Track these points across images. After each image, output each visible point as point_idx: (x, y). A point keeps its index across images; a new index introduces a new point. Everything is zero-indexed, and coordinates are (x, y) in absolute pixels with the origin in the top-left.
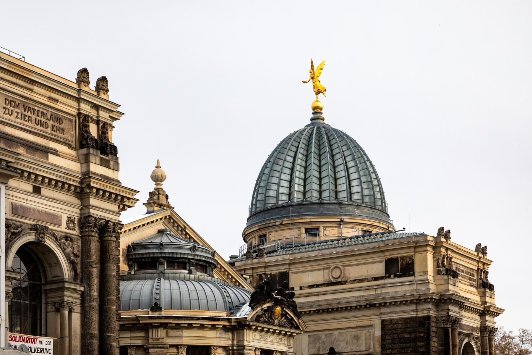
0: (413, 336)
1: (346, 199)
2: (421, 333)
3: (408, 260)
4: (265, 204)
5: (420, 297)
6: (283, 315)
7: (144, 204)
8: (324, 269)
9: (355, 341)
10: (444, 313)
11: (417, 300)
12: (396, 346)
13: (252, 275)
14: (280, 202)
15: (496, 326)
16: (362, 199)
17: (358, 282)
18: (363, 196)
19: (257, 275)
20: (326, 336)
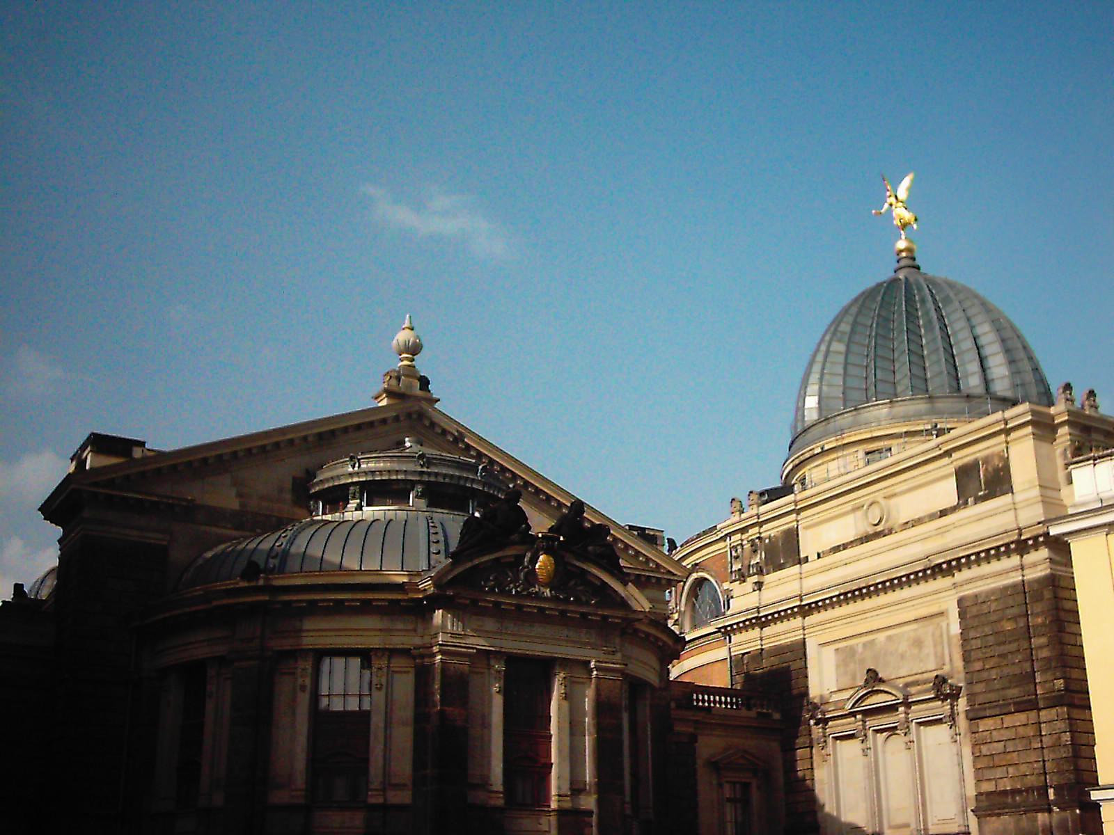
2: (1037, 615)
3: (996, 462)
5: (1021, 535)
7: (373, 398)
8: (855, 509)
9: (915, 651)
11: (1018, 542)
13: (741, 544)
19: (748, 541)
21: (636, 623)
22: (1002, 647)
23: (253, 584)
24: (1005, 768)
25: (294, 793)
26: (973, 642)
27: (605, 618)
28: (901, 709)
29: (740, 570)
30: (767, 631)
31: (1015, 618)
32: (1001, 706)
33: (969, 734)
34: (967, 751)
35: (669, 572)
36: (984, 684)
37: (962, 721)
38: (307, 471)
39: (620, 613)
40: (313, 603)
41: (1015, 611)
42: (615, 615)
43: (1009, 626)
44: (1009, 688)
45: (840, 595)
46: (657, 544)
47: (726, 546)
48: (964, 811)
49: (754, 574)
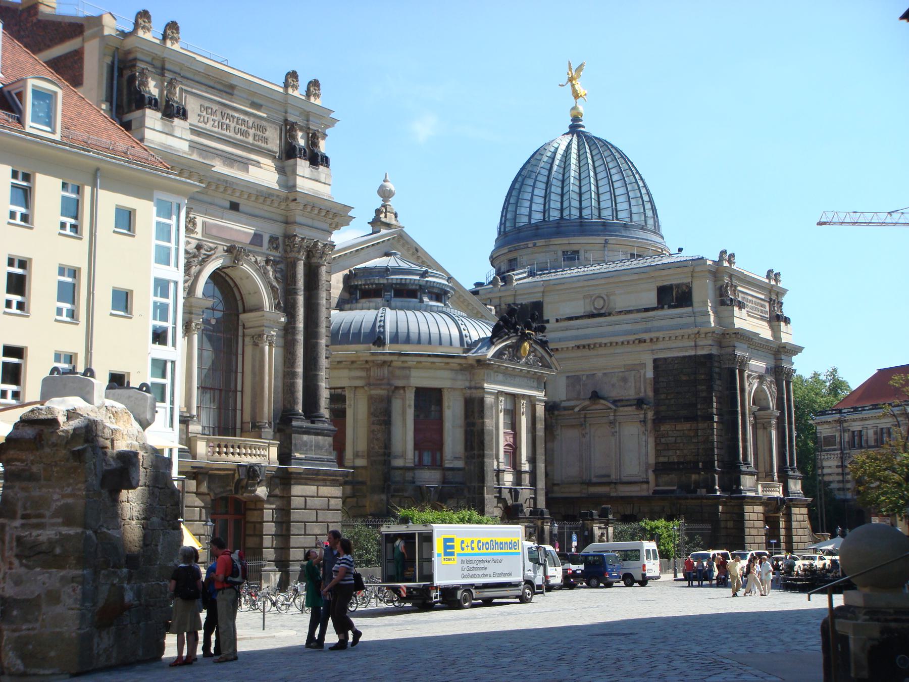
1: (611, 218)
3: (684, 288)
4: (515, 223)
6: (530, 352)
9: (622, 384)
10: (730, 350)
14: (533, 221)
15: (794, 367)
16: (631, 218)
18: (631, 213)
34: (651, 441)
37: (650, 425)
43: (684, 378)
48: (647, 471)
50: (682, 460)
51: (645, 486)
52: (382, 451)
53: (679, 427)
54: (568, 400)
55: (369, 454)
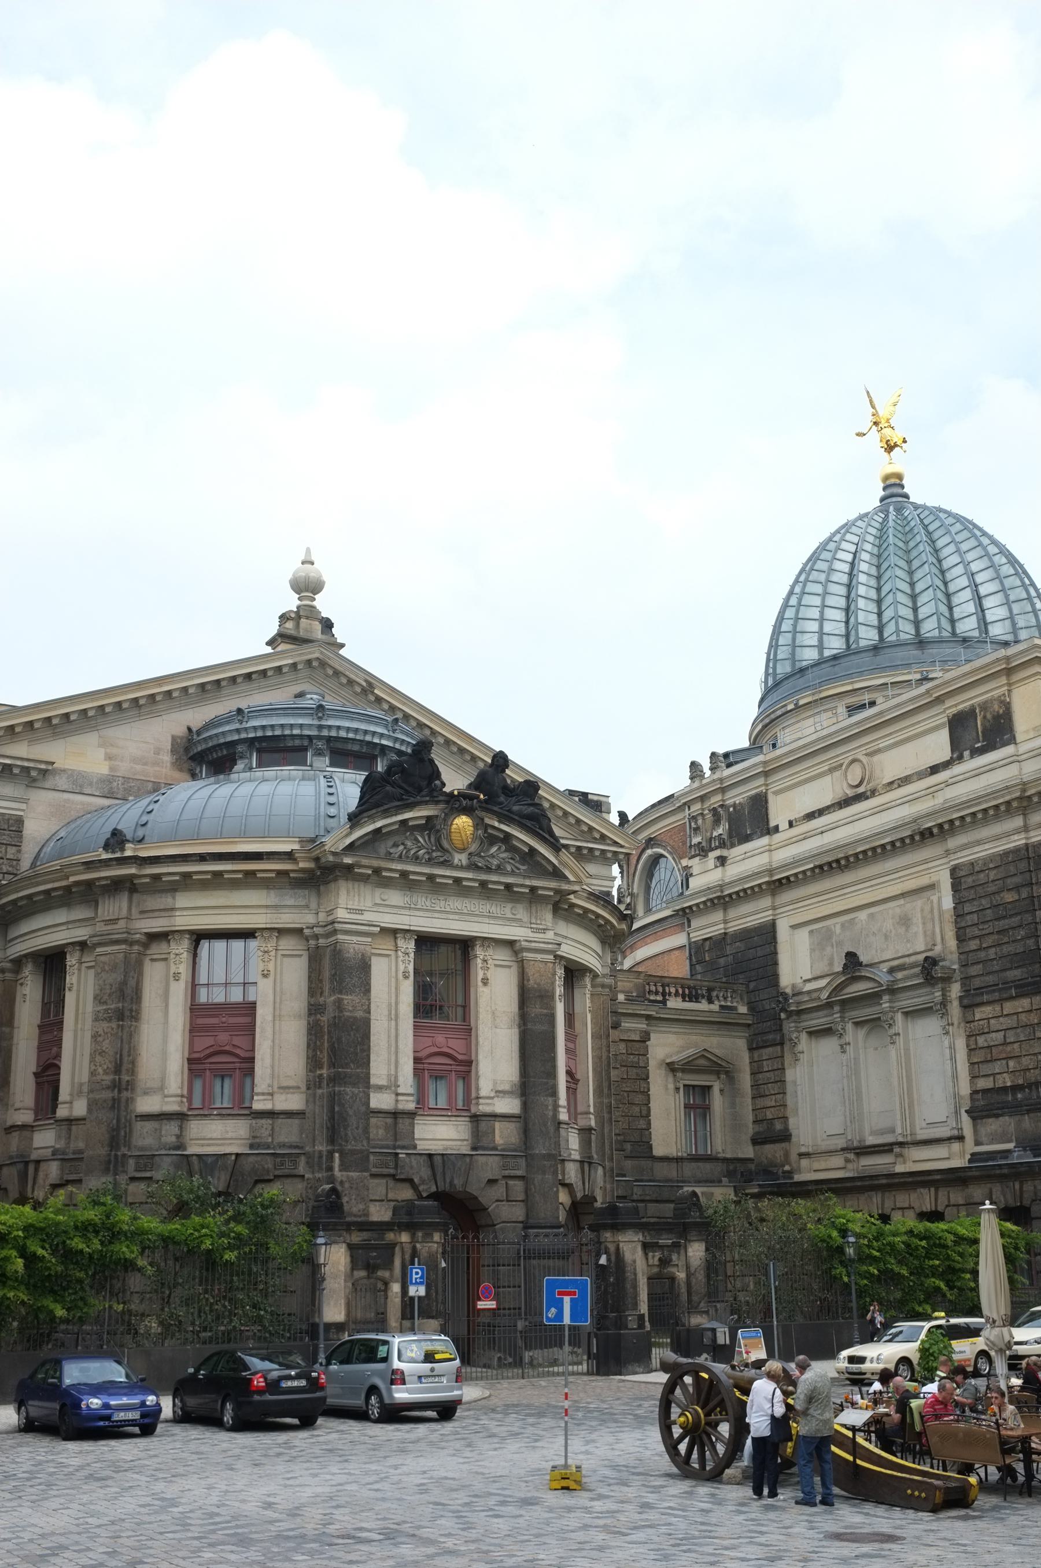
0: (1024, 895)
5: (1024, 791)
7: (268, 643)
8: (831, 770)
9: (902, 930)
11: (1020, 799)
12: (988, 928)
13: (702, 814)
17: (900, 786)
20: (843, 925)
21: (572, 896)
22: (1002, 922)
23: (118, 855)
24: (1004, 1062)
25: (166, 1099)
26: (968, 917)
27: (533, 889)
28: (886, 998)
29: (700, 843)
30: (732, 913)
31: (1017, 888)
32: (1000, 990)
33: (962, 1025)
34: (961, 1044)
35: (616, 843)
36: (981, 966)
37: (955, 1009)
38: (189, 729)
39: (553, 884)
40: (187, 876)
41: (1017, 880)
42: (546, 885)
43: (1009, 897)
44: (1011, 969)
45: (815, 867)
46: (601, 812)
47: (684, 818)
48: (957, 1113)
49: (716, 848)
50: (1021, 1082)
51: (956, 1146)
52: (108, 1078)
53: (1009, 1007)
54: (815, 979)
55: (94, 1085)
